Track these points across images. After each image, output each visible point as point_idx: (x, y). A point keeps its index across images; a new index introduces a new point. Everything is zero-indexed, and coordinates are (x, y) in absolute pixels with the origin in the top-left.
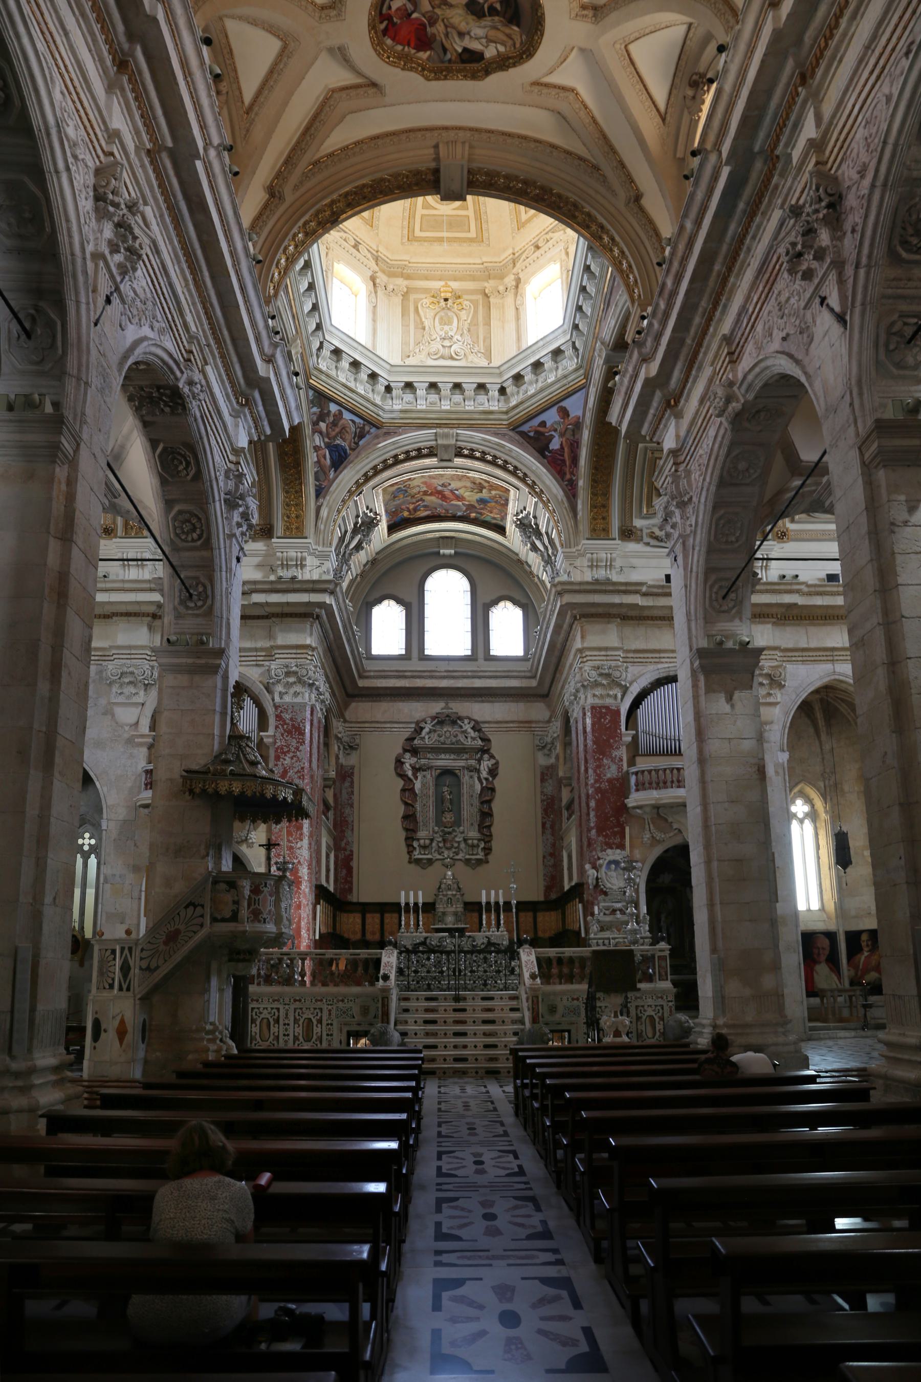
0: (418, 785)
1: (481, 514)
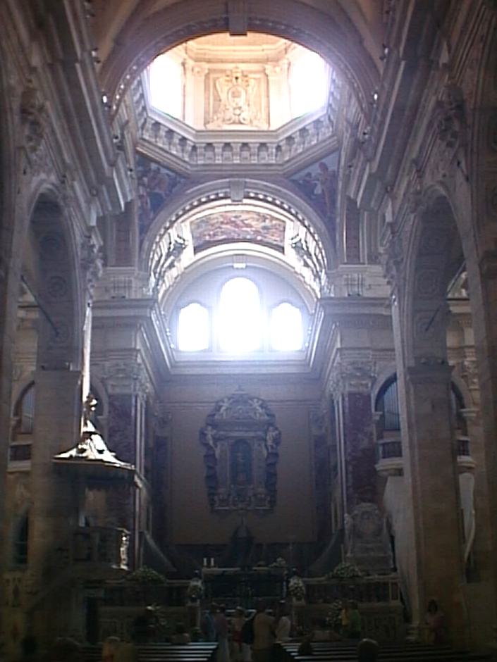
0: (217, 452)
1: (265, 237)
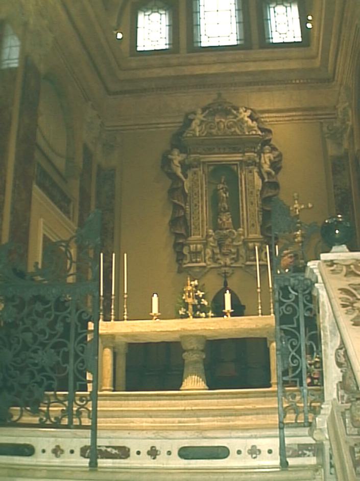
0: (187, 184)
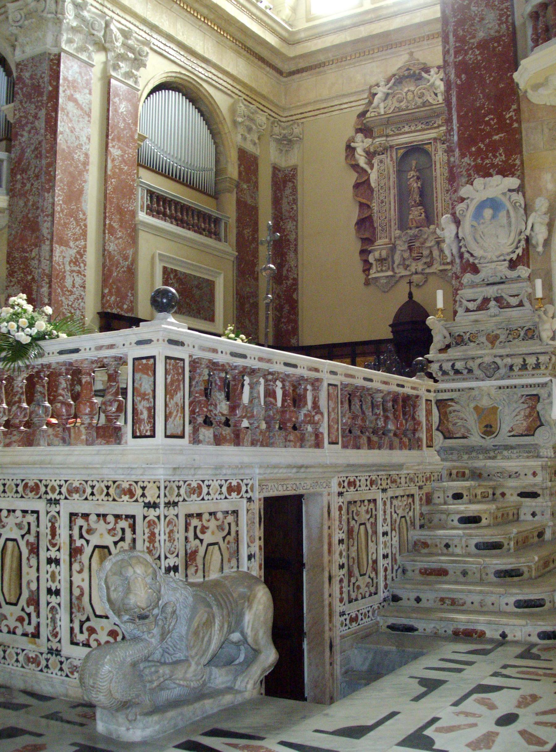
0: (373, 177)
